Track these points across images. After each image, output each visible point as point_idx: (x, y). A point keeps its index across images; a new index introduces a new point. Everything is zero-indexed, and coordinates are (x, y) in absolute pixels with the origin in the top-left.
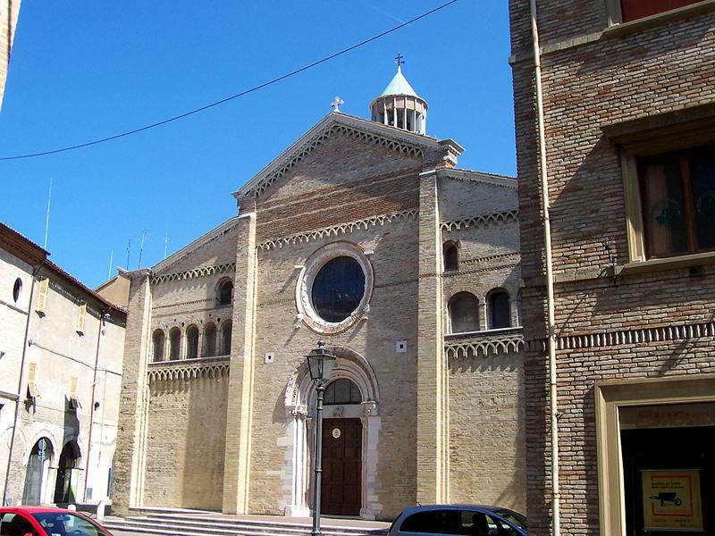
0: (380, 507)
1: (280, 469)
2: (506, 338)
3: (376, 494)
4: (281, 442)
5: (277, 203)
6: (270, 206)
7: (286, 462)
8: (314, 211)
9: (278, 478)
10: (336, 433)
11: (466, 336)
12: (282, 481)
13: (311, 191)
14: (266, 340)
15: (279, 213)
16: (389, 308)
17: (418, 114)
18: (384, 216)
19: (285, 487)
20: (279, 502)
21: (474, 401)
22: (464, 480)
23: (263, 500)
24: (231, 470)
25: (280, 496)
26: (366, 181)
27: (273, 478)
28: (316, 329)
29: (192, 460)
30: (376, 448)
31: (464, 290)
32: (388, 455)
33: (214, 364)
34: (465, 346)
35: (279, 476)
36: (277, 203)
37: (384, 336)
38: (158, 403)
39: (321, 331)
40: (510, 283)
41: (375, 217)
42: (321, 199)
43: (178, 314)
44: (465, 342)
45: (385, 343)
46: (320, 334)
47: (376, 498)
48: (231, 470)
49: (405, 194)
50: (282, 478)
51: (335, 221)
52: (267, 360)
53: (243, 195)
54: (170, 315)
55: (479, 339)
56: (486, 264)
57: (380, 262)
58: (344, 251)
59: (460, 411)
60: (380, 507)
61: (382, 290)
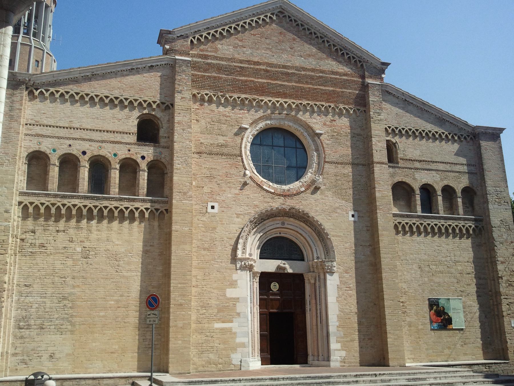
0: (343, 353)
1: (232, 322)
2: (436, 222)
3: (338, 342)
4: (231, 293)
5: (216, 58)
6: (207, 59)
7: (239, 314)
8: (260, 80)
9: (230, 330)
10: (275, 287)
11: (408, 216)
12: (235, 333)
13: (256, 59)
14: (206, 190)
15: (219, 69)
16: (340, 182)
17: (47, 7)
18: (332, 105)
19: (238, 340)
20: (233, 356)
21: (415, 267)
22: (412, 328)
23: (212, 356)
24: (180, 324)
25: (234, 350)
26: (313, 70)
27: (222, 330)
28: (264, 187)
29: (102, 314)
30: (336, 301)
31: (404, 180)
32: (348, 307)
33: (137, 205)
34: (407, 223)
35: (231, 329)
36: (216, 58)
37: (337, 205)
38: (38, 242)
39: (273, 191)
40: (436, 183)
41: (324, 103)
42: (267, 71)
43: (75, 139)
44: (407, 220)
45: (338, 211)
46: (271, 193)
47: (338, 346)
48: (180, 324)
49: (349, 93)
50: (234, 331)
51: (284, 95)
52: (210, 210)
53: (175, 36)
54: (58, 138)
55: (417, 219)
56: (417, 165)
57: (328, 142)
58: (264, 123)
59: (405, 273)
60: (343, 353)
61: (333, 166)
